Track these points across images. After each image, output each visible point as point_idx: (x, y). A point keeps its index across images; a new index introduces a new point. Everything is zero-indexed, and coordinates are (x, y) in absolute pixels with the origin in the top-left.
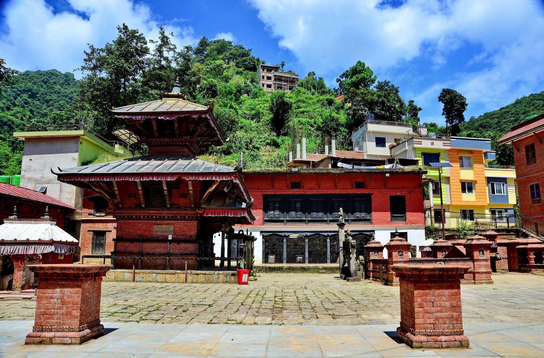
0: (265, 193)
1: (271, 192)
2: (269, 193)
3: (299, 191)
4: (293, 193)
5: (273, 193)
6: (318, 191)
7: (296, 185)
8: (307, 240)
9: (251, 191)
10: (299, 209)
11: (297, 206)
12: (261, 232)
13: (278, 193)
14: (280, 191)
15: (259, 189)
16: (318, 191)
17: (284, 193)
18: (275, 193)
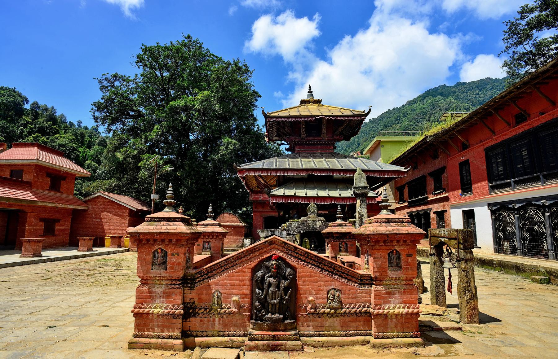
0: (486, 146)
1: (491, 143)
2: (490, 144)
3: (522, 127)
4: (516, 133)
5: (493, 143)
6: (550, 115)
7: (521, 118)
8: (547, 214)
9: (474, 148)
10: (526, 159)
11: (525, 153)
12: (489, 205)
13: (499, 140)
14: (500, 136)
15: (481, 142)
16: (550, 115)
17: (506, 137)
18: (497, 142)
